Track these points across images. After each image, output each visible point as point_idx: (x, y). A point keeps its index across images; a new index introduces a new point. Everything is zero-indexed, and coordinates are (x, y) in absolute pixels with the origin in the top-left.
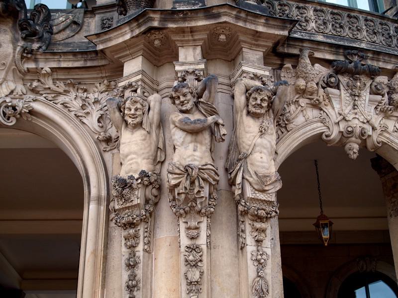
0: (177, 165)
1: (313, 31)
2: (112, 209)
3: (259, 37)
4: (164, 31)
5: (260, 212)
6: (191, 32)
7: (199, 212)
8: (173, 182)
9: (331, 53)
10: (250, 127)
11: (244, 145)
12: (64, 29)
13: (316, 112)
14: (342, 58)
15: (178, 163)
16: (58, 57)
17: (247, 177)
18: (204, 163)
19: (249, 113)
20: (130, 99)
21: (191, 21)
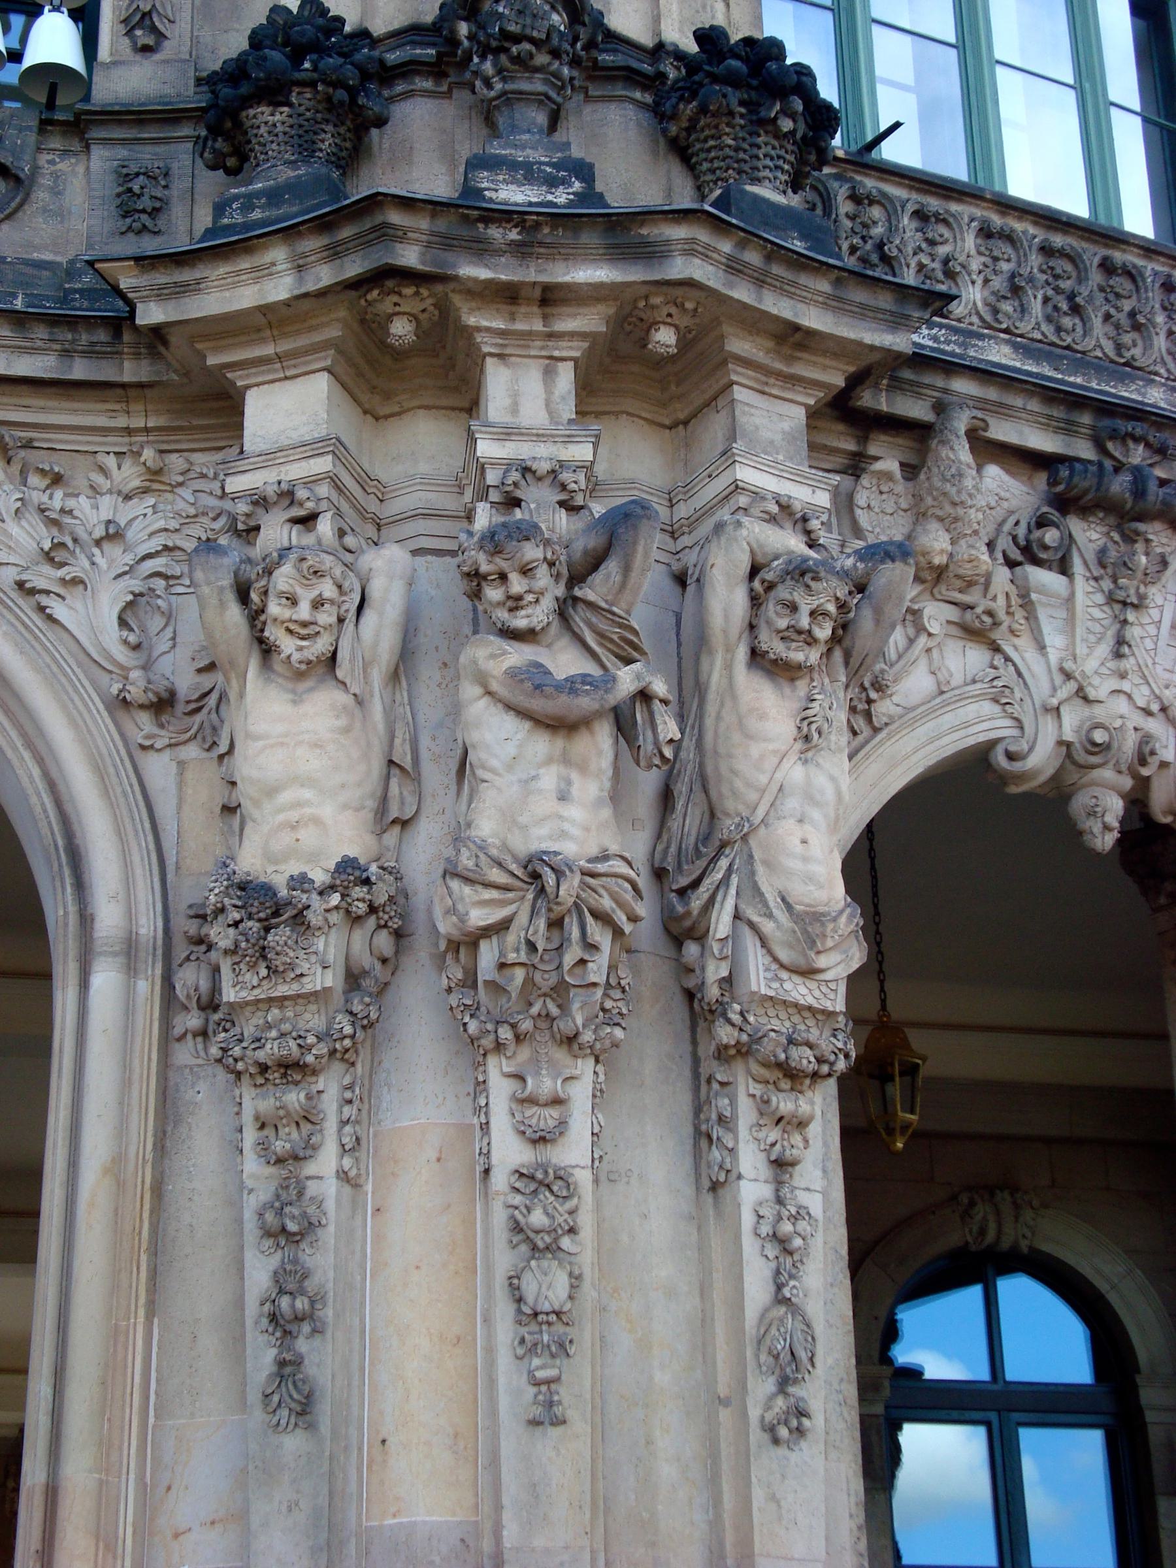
0: (494, 852)
1: (975, 319)
2: (188, 997)
3: (801, 346)
4: (439, 288)
5: (795, 1052)
7: (570, 1041)
8: (479, 917)
9: (1049, 425)
10: (763, 717)
11: (739, 784)
13: (976, 657)
14: (1084, 450)
15: (497, 842)
18: (594, 851)
20: (293, 557)
21: (550, 258)
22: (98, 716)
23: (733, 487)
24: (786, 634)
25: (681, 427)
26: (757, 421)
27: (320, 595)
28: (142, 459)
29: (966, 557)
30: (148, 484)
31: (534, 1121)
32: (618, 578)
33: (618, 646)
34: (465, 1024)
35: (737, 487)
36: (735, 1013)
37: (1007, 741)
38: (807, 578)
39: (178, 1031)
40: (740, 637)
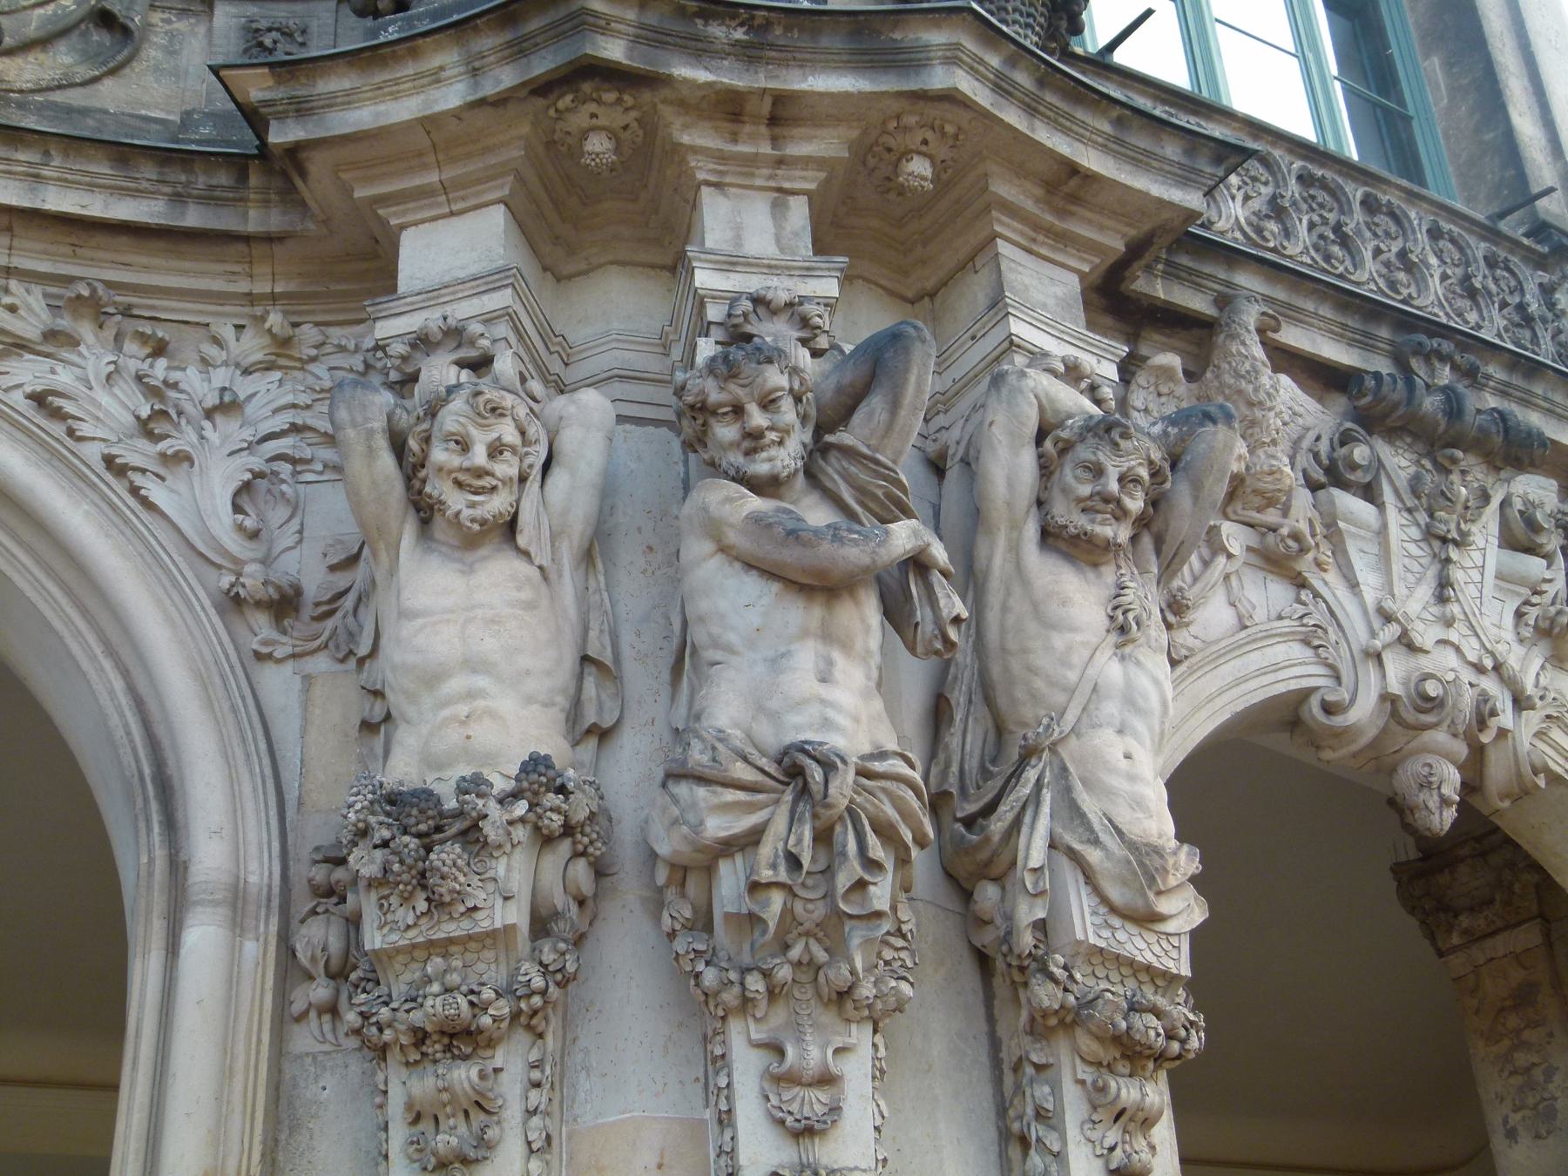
1: (1238, 235)
2: (313, 959)
3: (1074, 199)
4: (646, 96)
6: (773, 121)
7: (842, 996)
9: (1342, 335)
10: (1064, 603)
11: (1039, 684)
12: (43, 42)
13: (1278, 593)
14: (1383, 366)
16: (34, 157)
18: (867, 749)
19: (1050, 537)
21: (784, 63)
22: (202, 614)
23: (1006, 344)
24: (1089, 503)
25: (927, 299)
26: (1027, 281)
27: (499, 439)
28: (267, 325)
29: (1266, 468)
30: (274, 357)
31: (795, 1107)
32: (884, 417)
33: (882, 504)
34: (698, 975)
35: (1012, 343)
36: (1058, 966)
37: (1322, 691)
38: (1115, 434)
39: (298, 1007)
40: (1028, 512)
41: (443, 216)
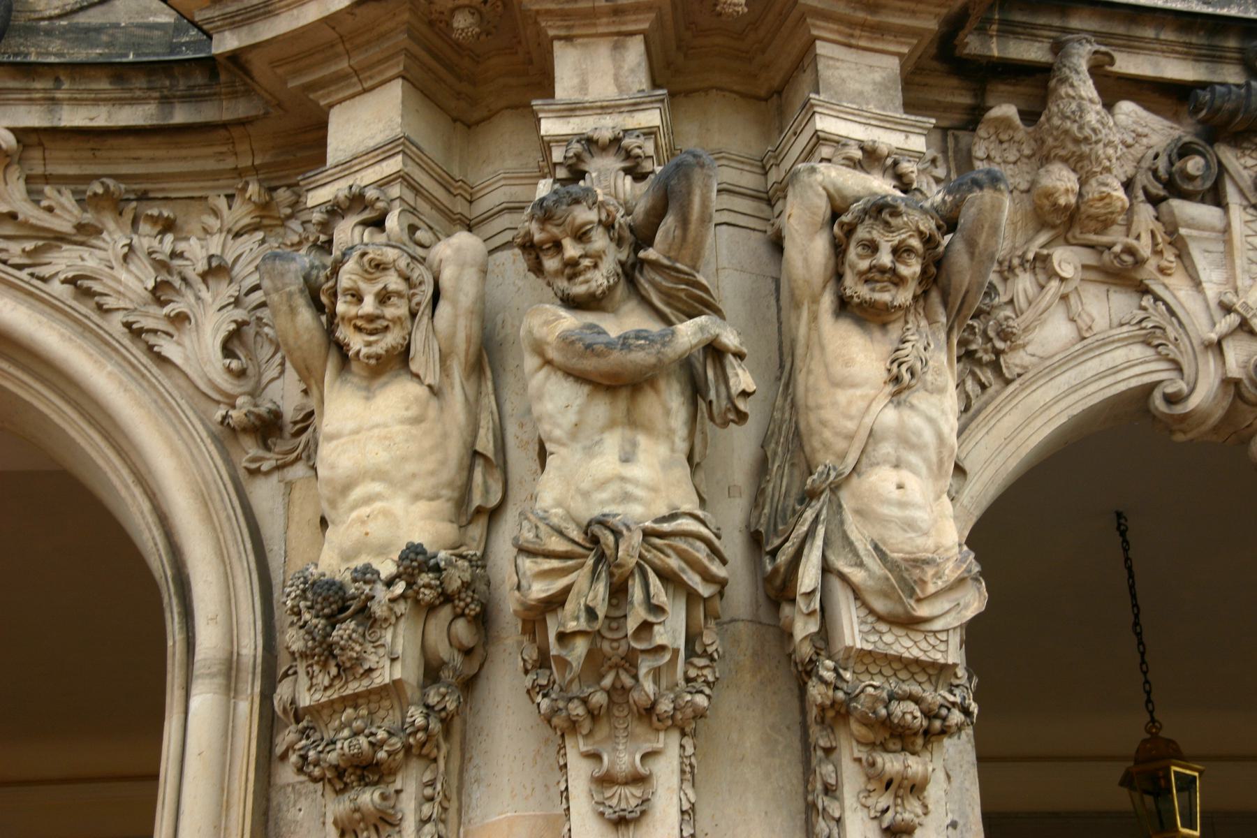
0: (555, 521)
2: (285, 710)
5: (898, 709)
7: (648, 713)
8: (539, 590)
10: (847, 363)
11: (827, 434)
13: (1122, 303)
14: (1232, 75)
15: (560, 511)
16: (49, 84)
17: (841, 564)
18: (664, 511)
19: (844, 306)
20: (356, 254)
22: (201, 444)
23: (814, 140)
24: (871, 275)
25: (775, 96)
26: (844, 74)
27: (385, 288)
28: (248, 195)
29: (1096, 196)
30: (258, 220)
31: (614, 802)
33: (685, 302)
34: (539, 704)
35: (818, 138)
36: (828, 670)
37: (1164, 384)
38: (885, 215)
39: (279, 750)
40: (824, 287)
41: (359, 94)
